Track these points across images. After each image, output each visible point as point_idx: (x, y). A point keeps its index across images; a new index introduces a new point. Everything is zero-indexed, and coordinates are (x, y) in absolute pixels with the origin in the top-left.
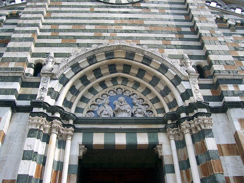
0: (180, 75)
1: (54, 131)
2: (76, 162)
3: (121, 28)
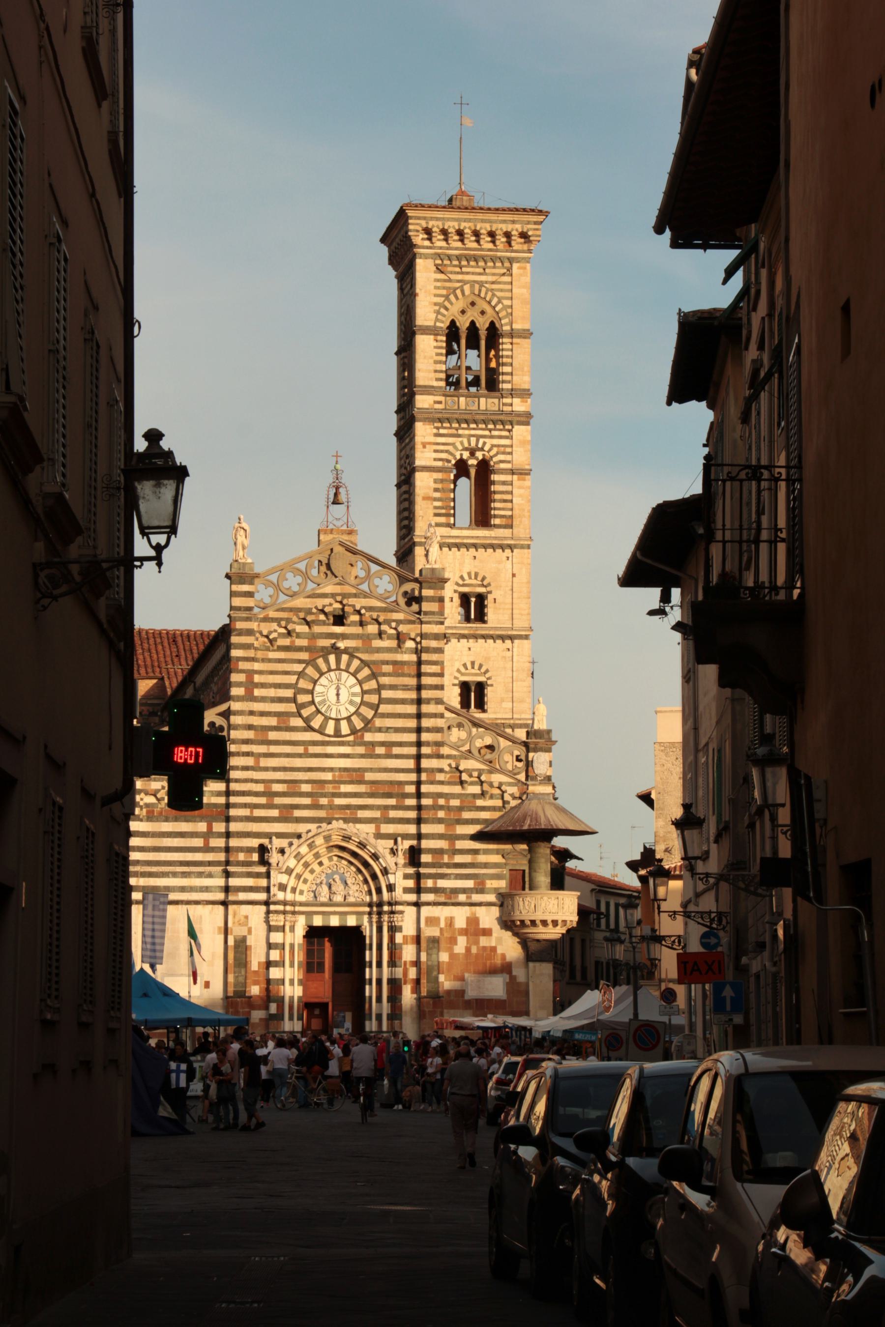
0: (388, 868)
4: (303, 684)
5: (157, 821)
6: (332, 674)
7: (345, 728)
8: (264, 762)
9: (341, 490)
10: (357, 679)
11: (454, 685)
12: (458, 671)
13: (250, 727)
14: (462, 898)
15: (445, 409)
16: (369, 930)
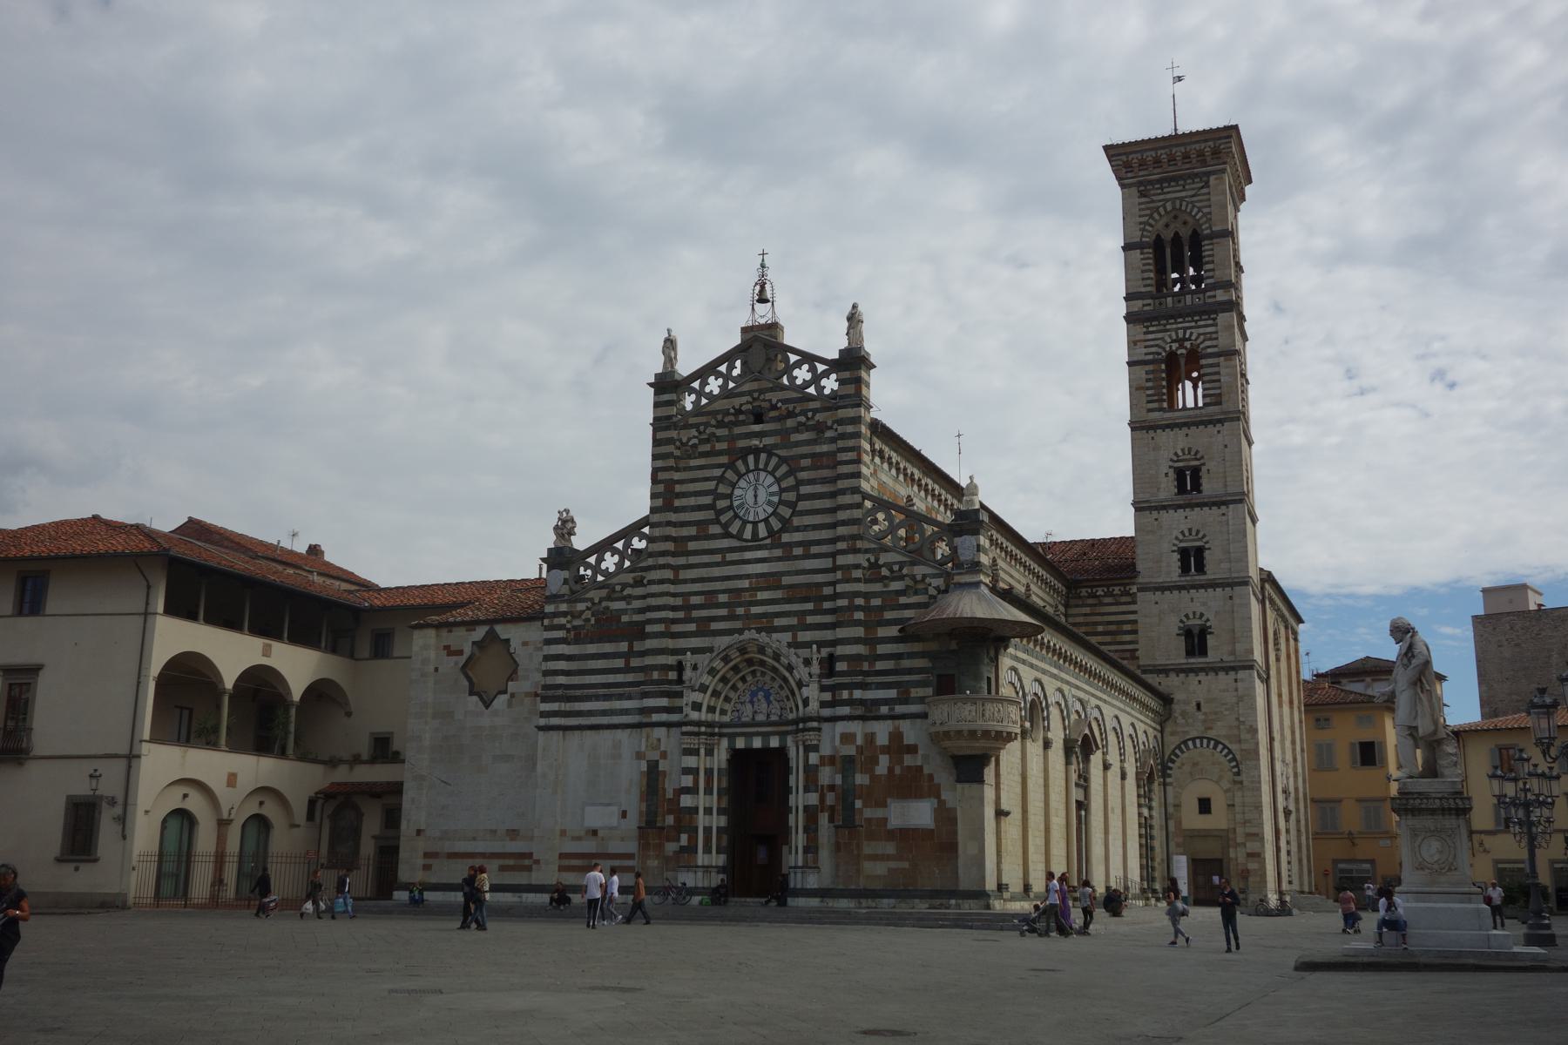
1: (701, 746)
2: (724, 765)
3: (756, 595)
4: (722, 489)
5: (583, 643)
6: (751, 475)
7: (762, 532)
8: (683, 575)
9: (768, 287)
10: (775, 477)
11: (1173, 551)
12: (1177, 538)
13: (667, 538)
14: (884, 710)
16: (792, 753)
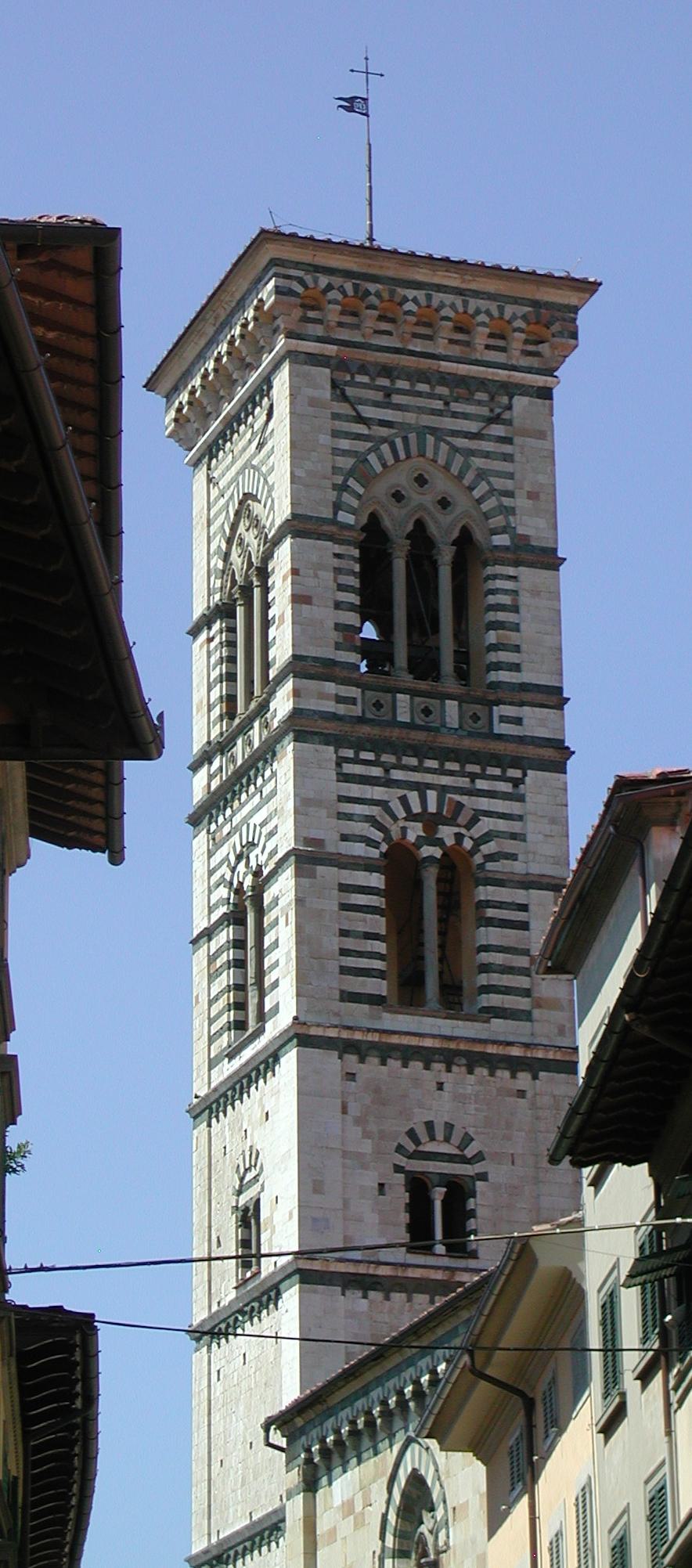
15: (361, 720)
